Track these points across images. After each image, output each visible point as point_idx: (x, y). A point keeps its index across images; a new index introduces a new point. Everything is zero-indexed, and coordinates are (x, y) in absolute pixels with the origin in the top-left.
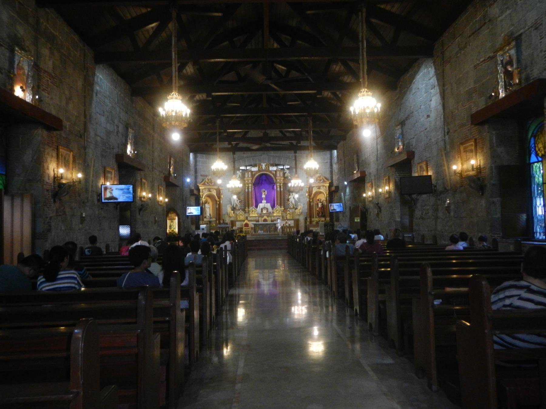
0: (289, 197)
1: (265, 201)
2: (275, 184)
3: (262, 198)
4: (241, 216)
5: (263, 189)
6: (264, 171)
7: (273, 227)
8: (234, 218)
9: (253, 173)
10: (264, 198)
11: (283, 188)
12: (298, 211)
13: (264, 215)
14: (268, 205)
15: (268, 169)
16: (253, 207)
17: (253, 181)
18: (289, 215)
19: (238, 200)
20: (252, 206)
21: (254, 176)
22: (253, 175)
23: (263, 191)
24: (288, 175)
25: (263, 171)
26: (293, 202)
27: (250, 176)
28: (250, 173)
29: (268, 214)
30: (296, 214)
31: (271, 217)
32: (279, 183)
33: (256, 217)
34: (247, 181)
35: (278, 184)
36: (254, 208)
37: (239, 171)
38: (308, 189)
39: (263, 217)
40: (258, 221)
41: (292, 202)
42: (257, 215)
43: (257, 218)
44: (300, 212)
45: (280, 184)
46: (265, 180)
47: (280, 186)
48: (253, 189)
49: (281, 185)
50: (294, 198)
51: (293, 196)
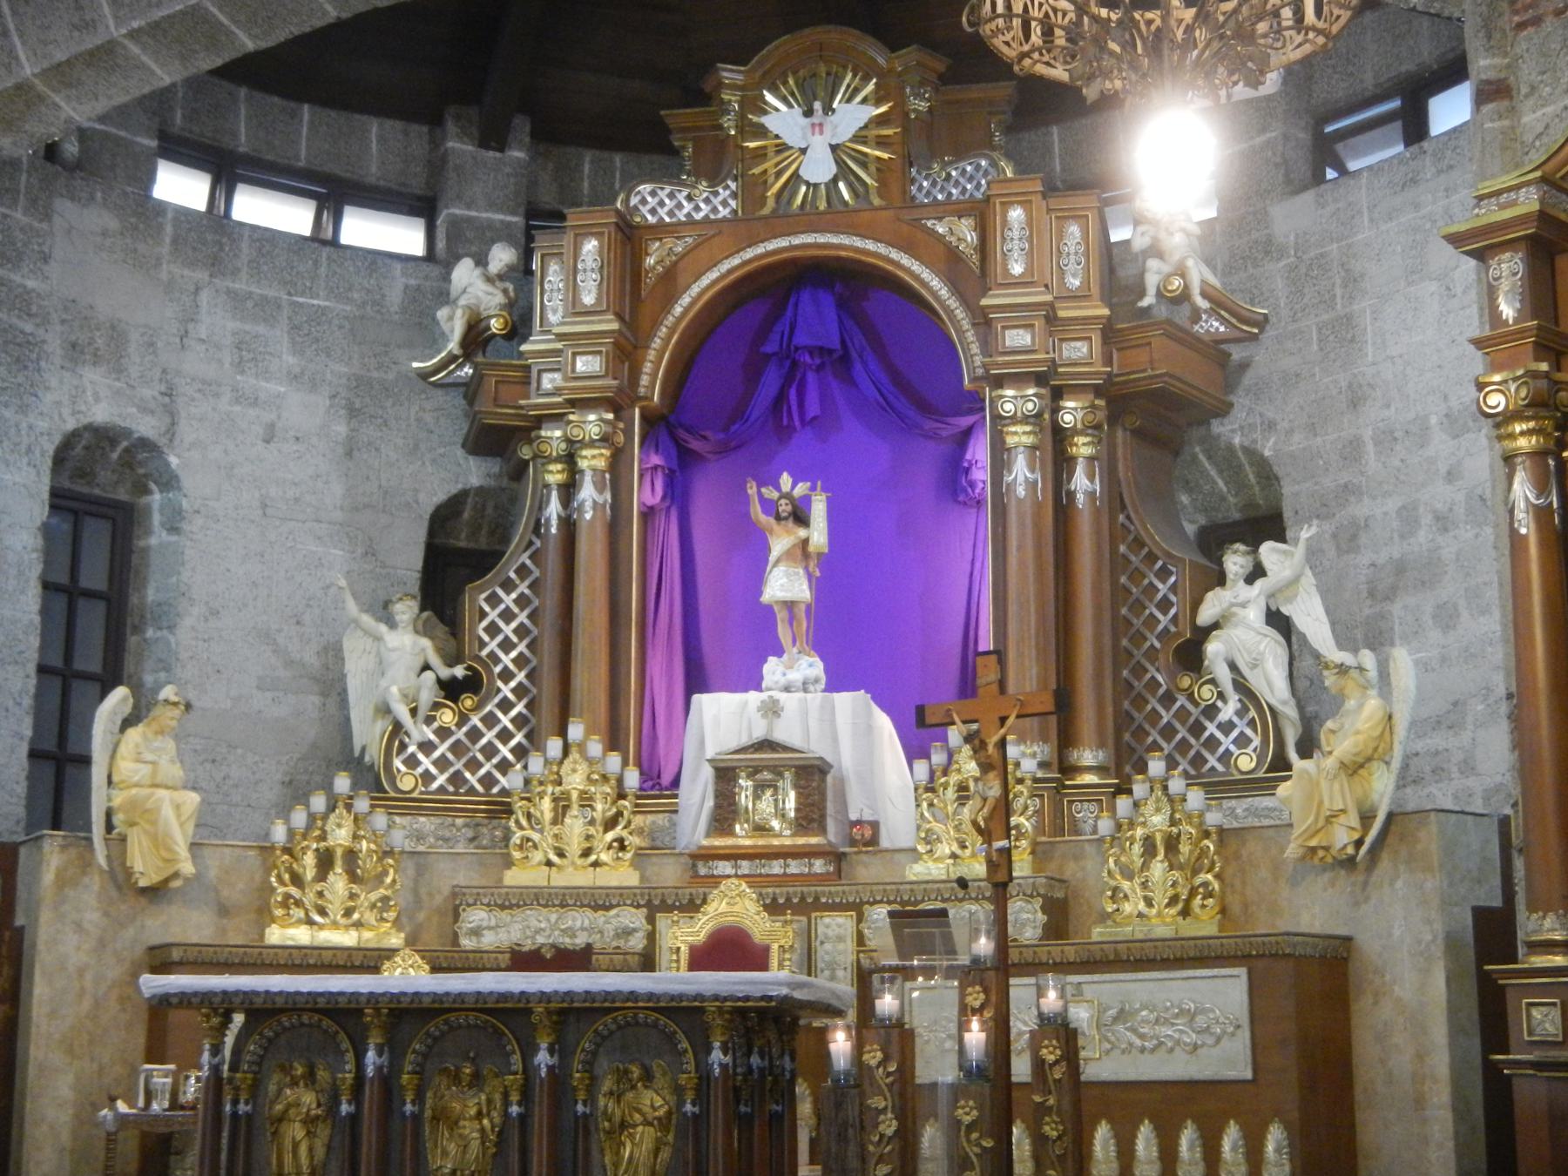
0: (1206, 615)
1: (811, 667)
2: (974, 403)
3: (769, 609)
4: (338, 883)
5: (786, 480)
6: (836, 217)
7: (653, 1101)
8: (223, 911)
9: (650, 261)
10: (790, 605)
11: (1107, 464)
12: (1336, 795)
13: (715, 881)
14: (829, 713)
15: (877, 201)
16: (576, 731)
17: (652, 381)
18: (1158, 868)
19: (435, 660)
20: (563, 733)
21: (670, 299)
22: (649, 281)
23: (769, 507)
24: (1184, 297)
25: (809, 219)
26: (1273, 683)
27: (588, 299)
28: (590, 246)
29: (819, 866)
30: (1292, 850)
31: (857, 908)
32: (1040, 379)
33: (600, 901)
34: (549, 381)
35: (1011, 401)
36: (595, 748)
37: (481, 261)
38: (1509, 268)
39: (692, 907)
40: (648, 962)
41: (1255, 681)
42: (630, 878)
43: (633, 918)
44: (1366, 818)
45: (1058, 394)
46: (840, 361)
47: (1060, 437)
48: (644, 493)
49: (1072, 412)
50: (1279, 621)
51: (1271, 596)
